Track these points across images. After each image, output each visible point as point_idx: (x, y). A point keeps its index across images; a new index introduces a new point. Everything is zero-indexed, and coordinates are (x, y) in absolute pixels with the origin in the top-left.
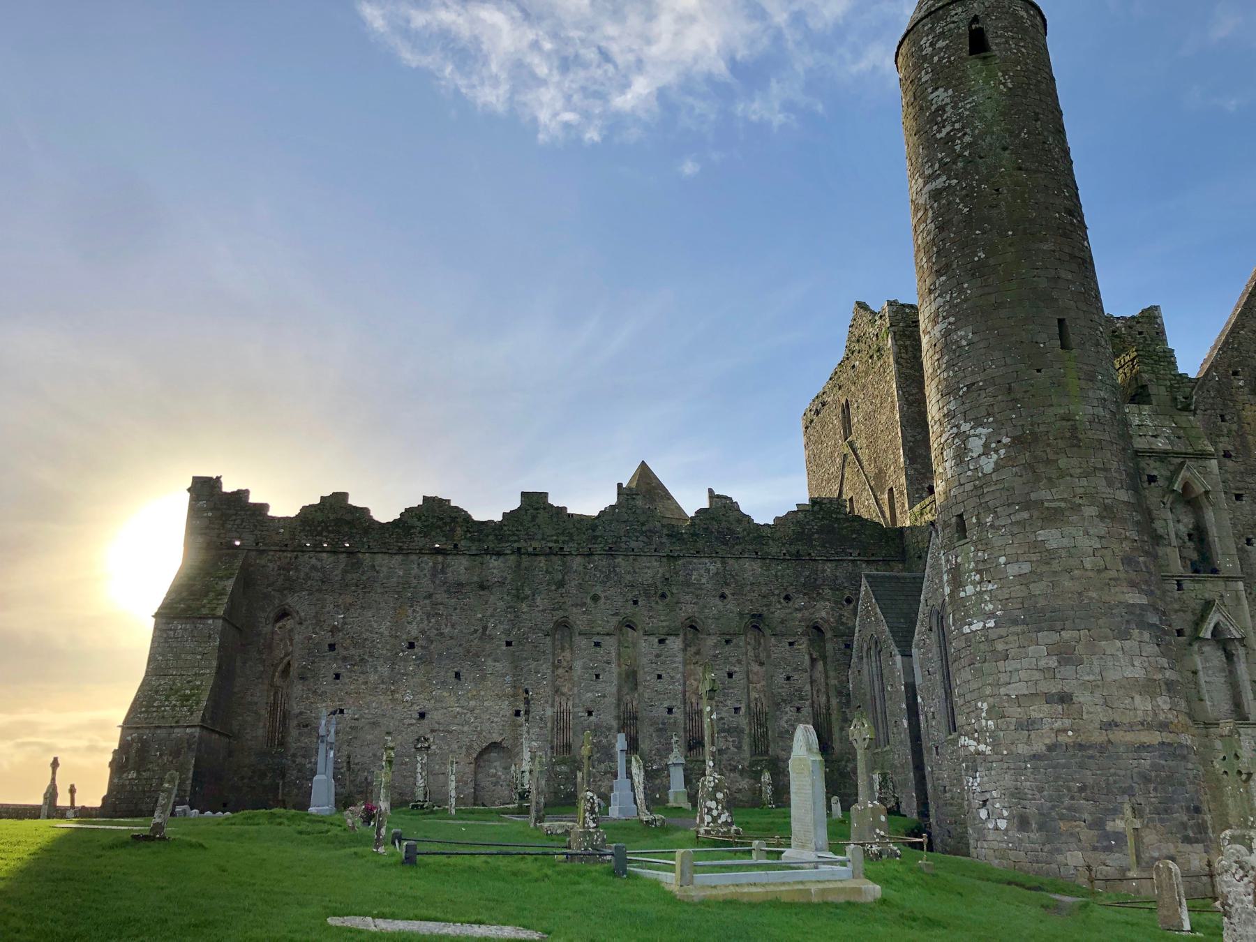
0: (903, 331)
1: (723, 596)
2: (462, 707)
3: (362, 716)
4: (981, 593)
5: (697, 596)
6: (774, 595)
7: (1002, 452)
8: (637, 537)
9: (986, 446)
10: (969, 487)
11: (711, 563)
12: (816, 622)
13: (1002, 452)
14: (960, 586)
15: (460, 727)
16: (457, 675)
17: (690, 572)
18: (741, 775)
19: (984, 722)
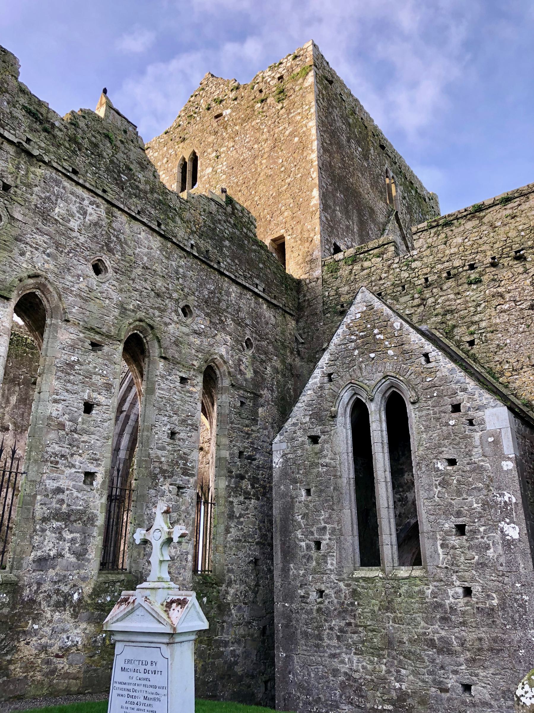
1: (98, 269)
5: (58, 245)
6: (171, 298)
11: (92, 203)
12: (213, 360)
17: (53, 198)
18: (75, 615)
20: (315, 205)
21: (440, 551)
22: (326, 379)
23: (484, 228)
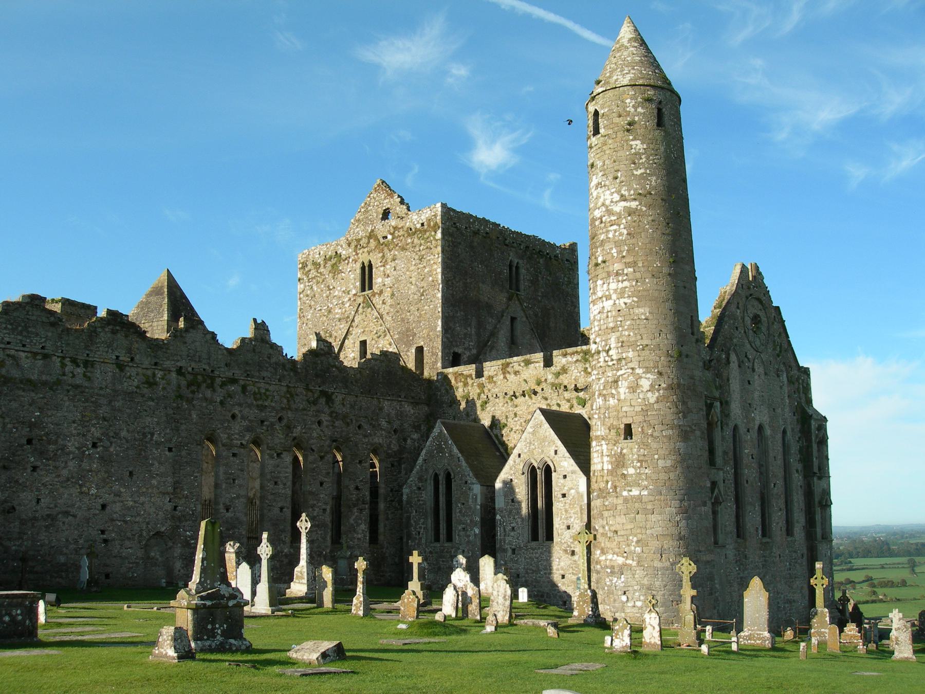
0: (448, 229)
2: (135, 502)
3: (56, 506)
4: (639, 474)
7: (661, 392)
8: (267, 368)
9: (651, 386)
10: (638, 409)
13: (661, 392)
14: (623, 466)
15: (133, 518)
16: (131, 474)
19: (633, 548)
20: (439, 331)
21: (457, 537)
22: (424, 462)
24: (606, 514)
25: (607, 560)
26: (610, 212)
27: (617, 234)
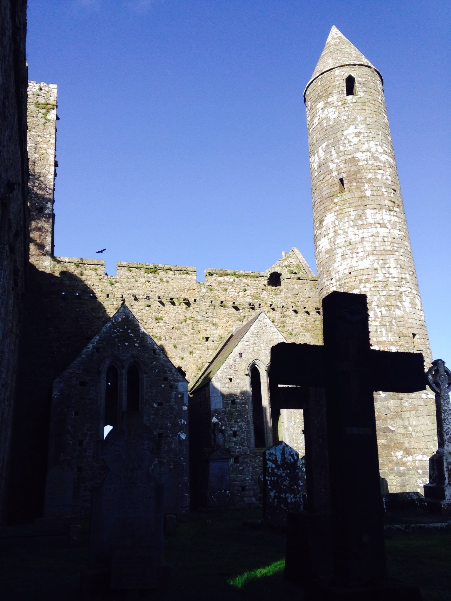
10: (419, 322)
23: (158, 279)
24: (407, 414)
25: (416, 460)
26: (376, 159)
27: (385, 177)
